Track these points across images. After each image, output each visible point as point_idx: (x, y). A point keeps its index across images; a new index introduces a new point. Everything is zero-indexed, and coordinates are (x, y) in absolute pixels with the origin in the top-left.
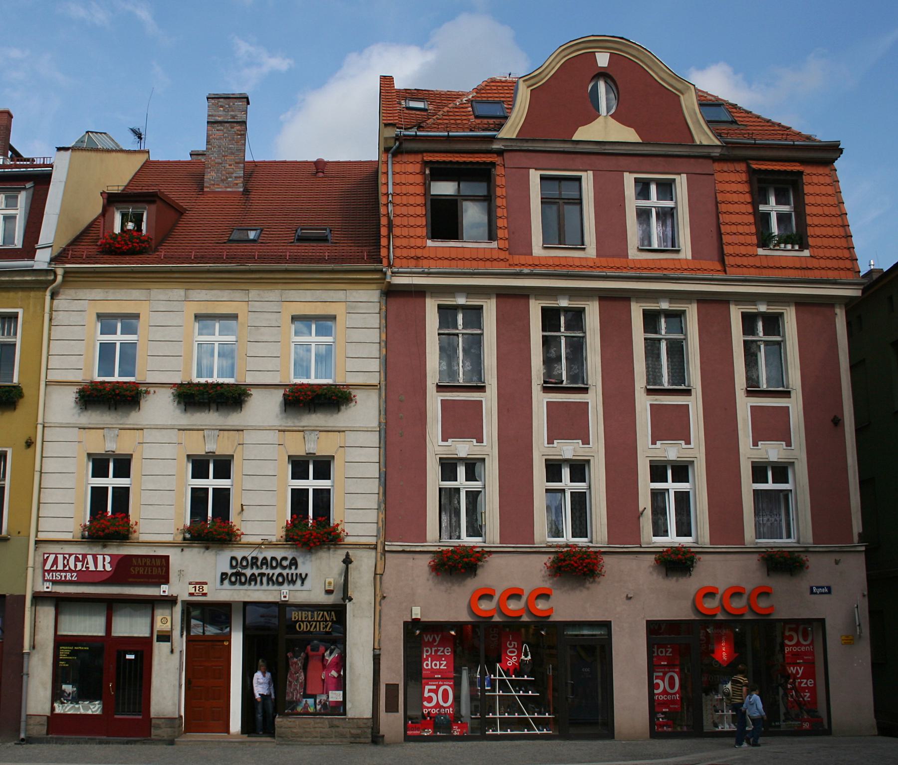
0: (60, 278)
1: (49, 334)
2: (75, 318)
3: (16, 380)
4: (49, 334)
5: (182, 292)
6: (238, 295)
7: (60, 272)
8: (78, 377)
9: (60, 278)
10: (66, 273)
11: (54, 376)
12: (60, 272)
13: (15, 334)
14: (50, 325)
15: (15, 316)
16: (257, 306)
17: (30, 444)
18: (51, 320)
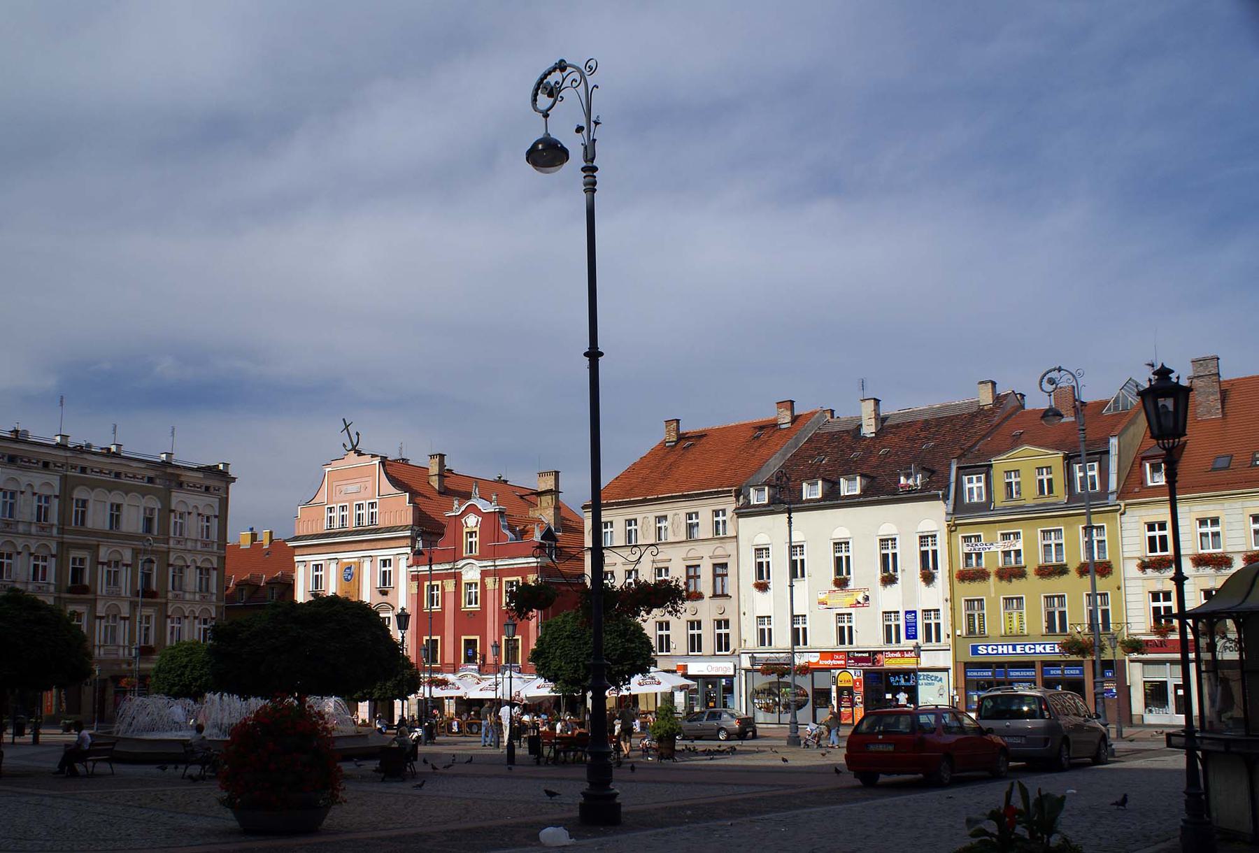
0: (1123, 508)
1: (1121, 535)
2: (1133, 525)
3: (1108, 558)
4: (1121, 535)
5: (1187, 508)
6: (1218, 507)
7: (1122, 504)
8: (1139, 555)
9: (1123, 508)
10: (1126, 505)
11: (1126, 555)
12: (1122, 504)
13: (1104, 535)
14: (1121, 530)
15: (1103, 527)
16: (1229, 512)
17: (1119, 588)
18: (1121, 527)
